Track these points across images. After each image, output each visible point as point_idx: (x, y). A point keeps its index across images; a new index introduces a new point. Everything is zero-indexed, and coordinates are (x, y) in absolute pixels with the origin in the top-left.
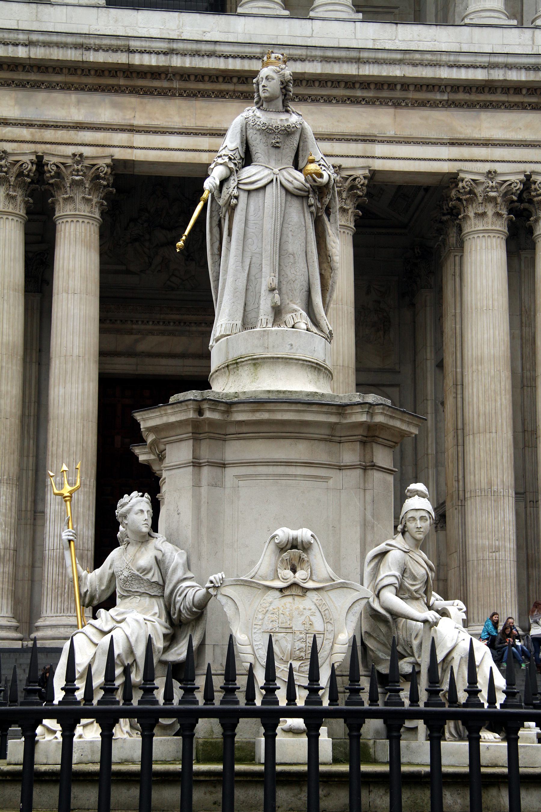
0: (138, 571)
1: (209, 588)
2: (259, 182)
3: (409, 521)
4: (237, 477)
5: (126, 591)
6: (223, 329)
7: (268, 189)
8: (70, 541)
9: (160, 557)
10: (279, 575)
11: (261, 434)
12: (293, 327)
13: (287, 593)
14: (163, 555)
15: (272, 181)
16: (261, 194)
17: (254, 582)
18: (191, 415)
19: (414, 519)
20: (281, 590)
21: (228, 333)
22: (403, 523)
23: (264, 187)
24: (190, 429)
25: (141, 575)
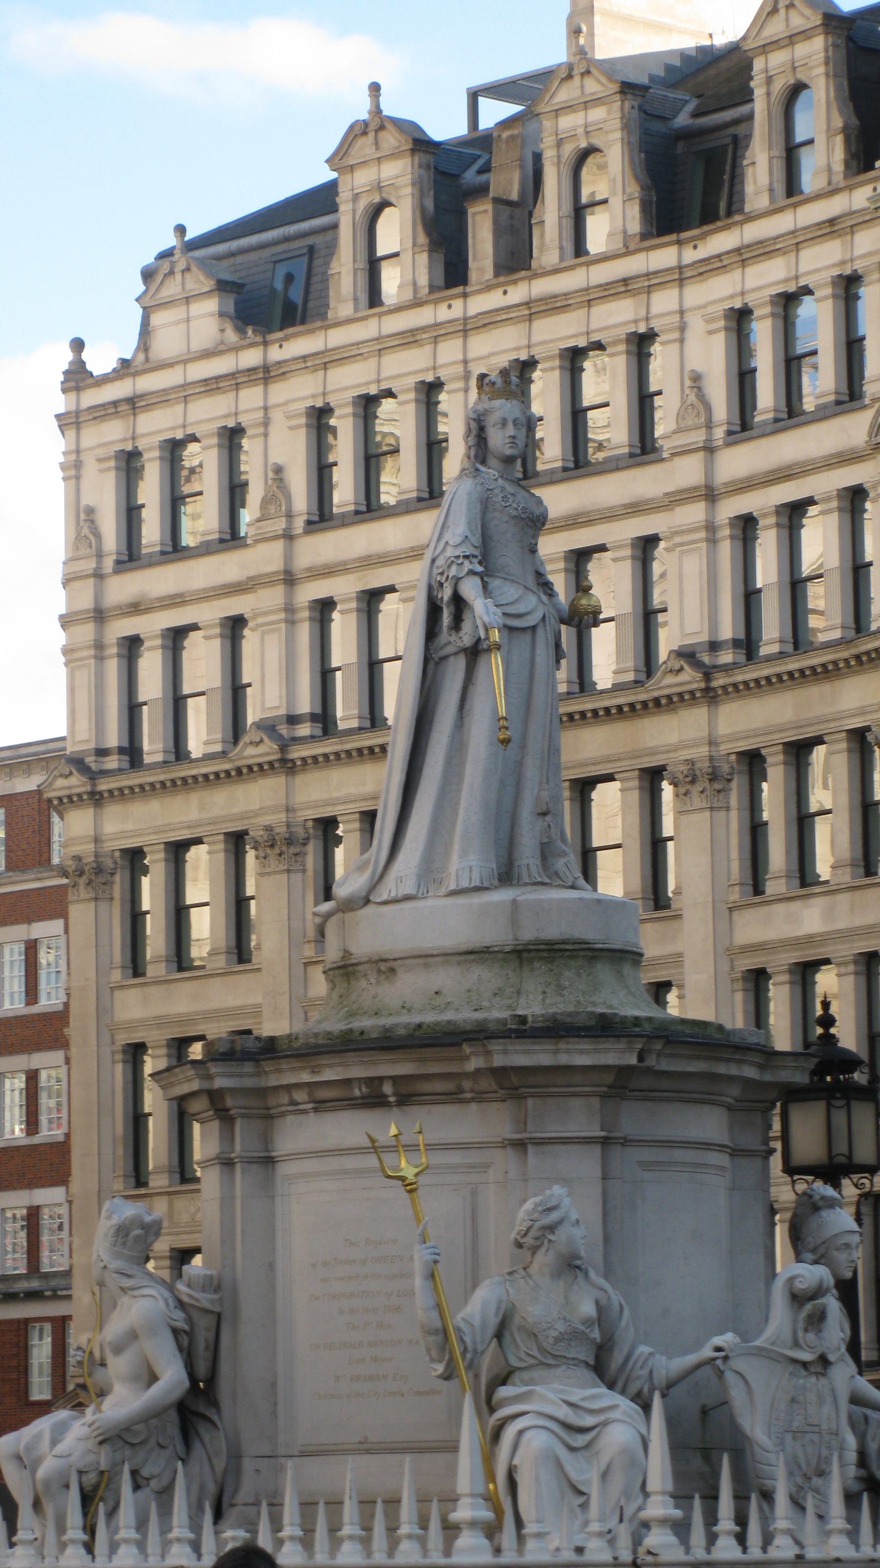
0: (583, 1324)
1: (714, 1359)
2: (529, 617)
3: (837, 1249)
4: (641, 1164)
5: (554, 1356)
6: (476, 875)
7: (540, 632)
8: (436, 1262)
9: (604, 1302)
10: (801, 1341)
11: (683, 1095)
12: (573, 887)
13: (812, 1369)
14: (609, 1298)
15: (544, 617)
16: (527, 637)
17: (773, 1351)
18: (633, 1061)
19: (847, 1246)
20: (805, 1365)
21: (485, 885)
22: (822, 1250)
23: (534, 628)
24: (609, 1079)
25: (587, 1331)
